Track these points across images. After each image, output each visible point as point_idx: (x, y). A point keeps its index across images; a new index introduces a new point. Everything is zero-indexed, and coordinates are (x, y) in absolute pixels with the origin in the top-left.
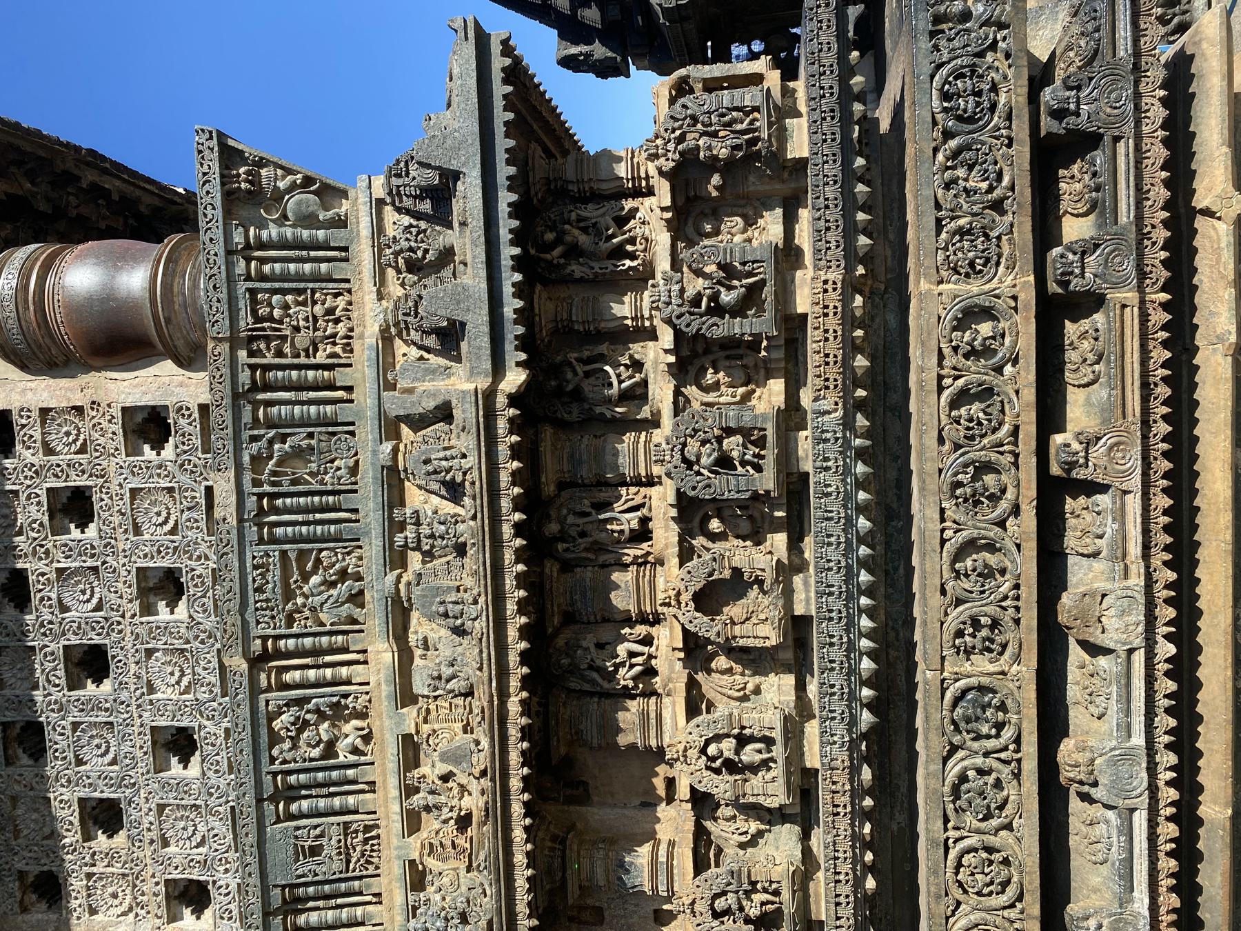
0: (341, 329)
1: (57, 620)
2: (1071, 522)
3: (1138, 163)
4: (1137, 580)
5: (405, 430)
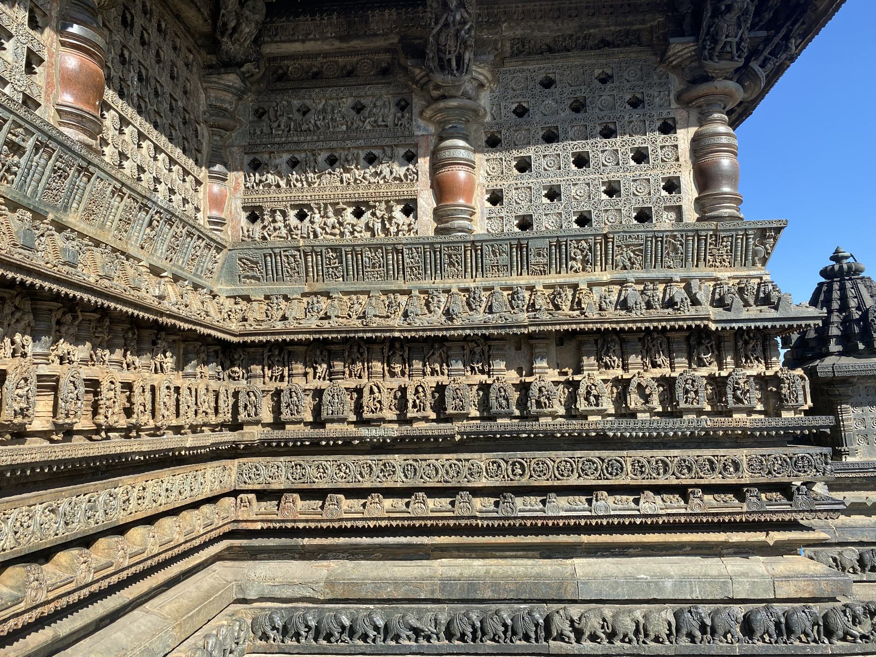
0: (718, 264)
1: (597, 148)
2: (671, 496)
3: (783, 511)
4: (660, 512)
5: (683, 285)
